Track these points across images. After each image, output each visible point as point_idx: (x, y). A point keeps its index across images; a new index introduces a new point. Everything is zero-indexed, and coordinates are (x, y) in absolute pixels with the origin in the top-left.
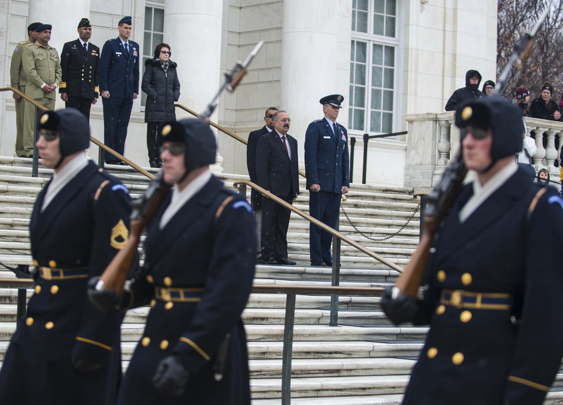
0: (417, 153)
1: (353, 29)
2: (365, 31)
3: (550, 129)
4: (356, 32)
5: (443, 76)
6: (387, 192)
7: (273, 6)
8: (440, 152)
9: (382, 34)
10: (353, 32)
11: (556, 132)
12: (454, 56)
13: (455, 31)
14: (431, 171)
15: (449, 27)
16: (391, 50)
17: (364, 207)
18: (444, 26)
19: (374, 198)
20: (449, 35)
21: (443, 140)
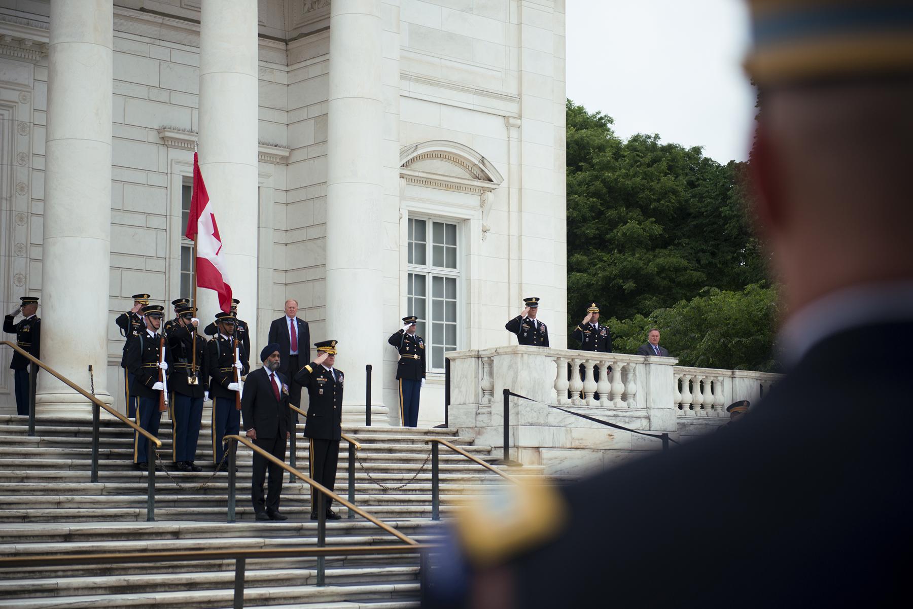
0: (460, 391)
1: (410, 261)
2: (424, 263)
3: (601, 361)
4: (414, 265)
5: (509, 307)
6: (428, 434)
7: (318, 241)
8: (484, 390)
9: (443, 266)
10: (410, 265)
11: (607, 364)
12: (520, 285)
13: (520, 259)
14: (474, 410)
15: (514, 255)
16: (454, 280)
17: (401, 451)
18: (509, 254)
19: (413, 441)
20: (514, 263)
21: (486, 377)
